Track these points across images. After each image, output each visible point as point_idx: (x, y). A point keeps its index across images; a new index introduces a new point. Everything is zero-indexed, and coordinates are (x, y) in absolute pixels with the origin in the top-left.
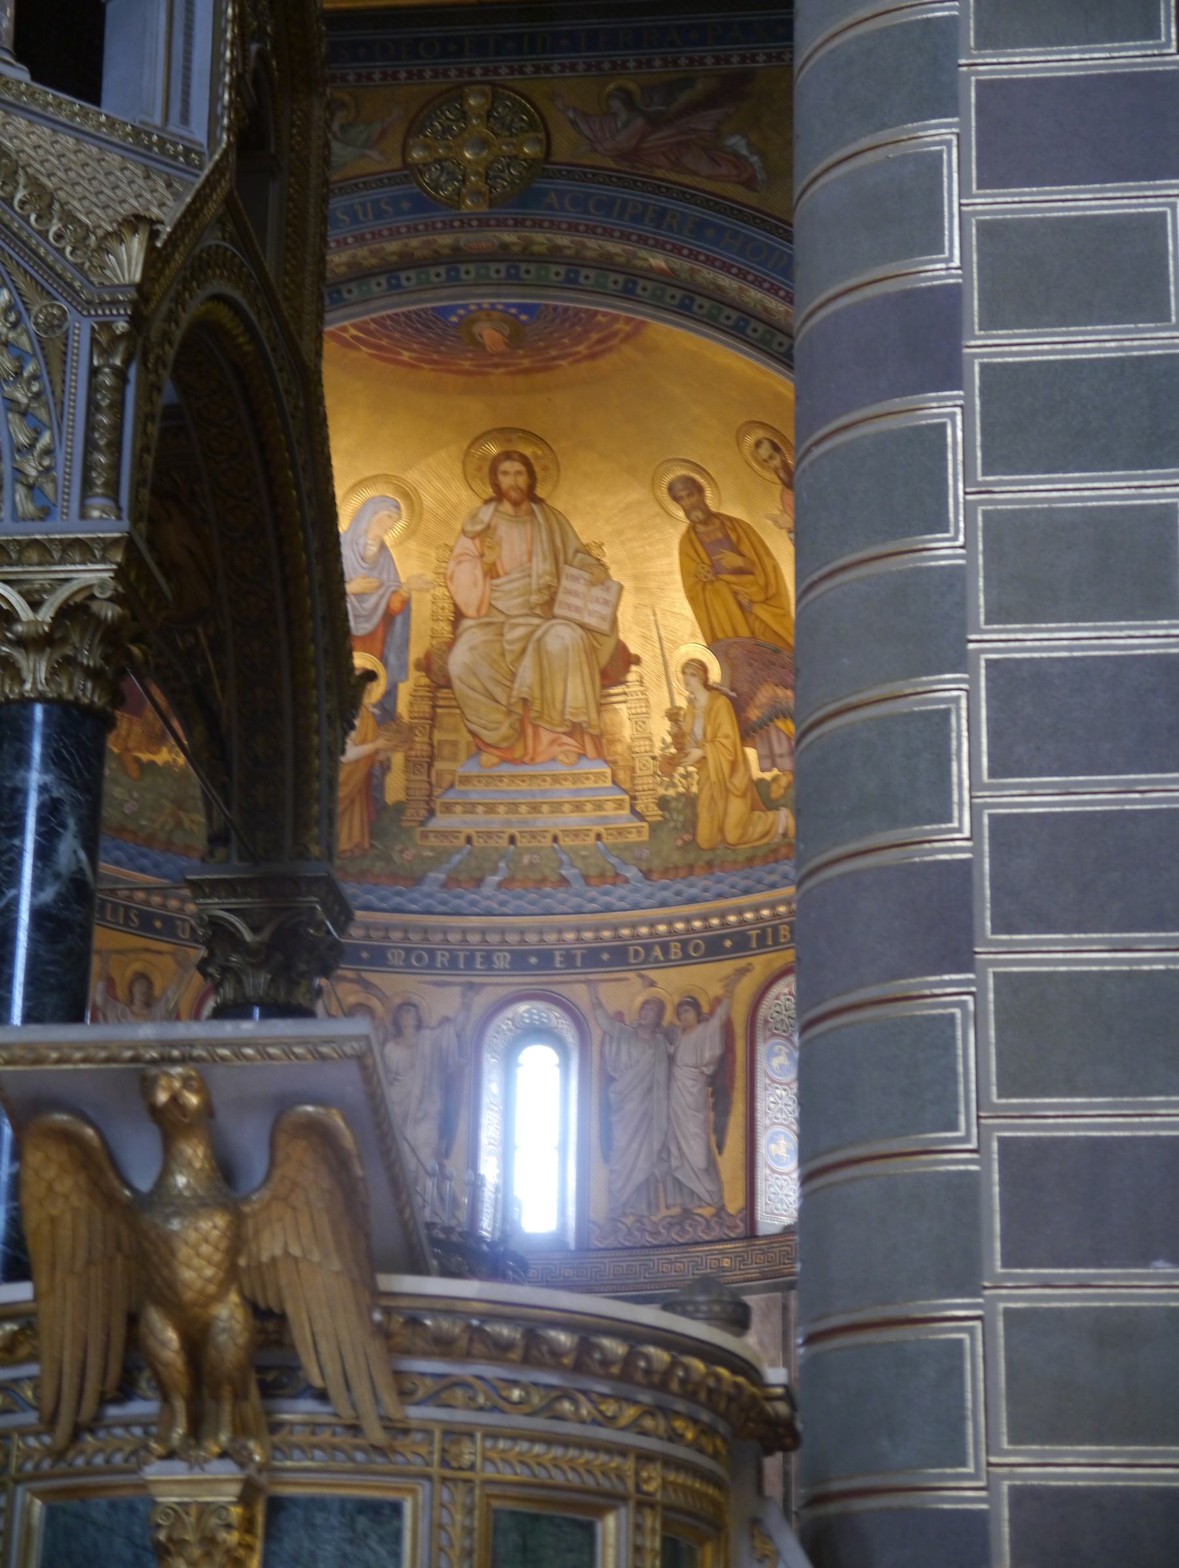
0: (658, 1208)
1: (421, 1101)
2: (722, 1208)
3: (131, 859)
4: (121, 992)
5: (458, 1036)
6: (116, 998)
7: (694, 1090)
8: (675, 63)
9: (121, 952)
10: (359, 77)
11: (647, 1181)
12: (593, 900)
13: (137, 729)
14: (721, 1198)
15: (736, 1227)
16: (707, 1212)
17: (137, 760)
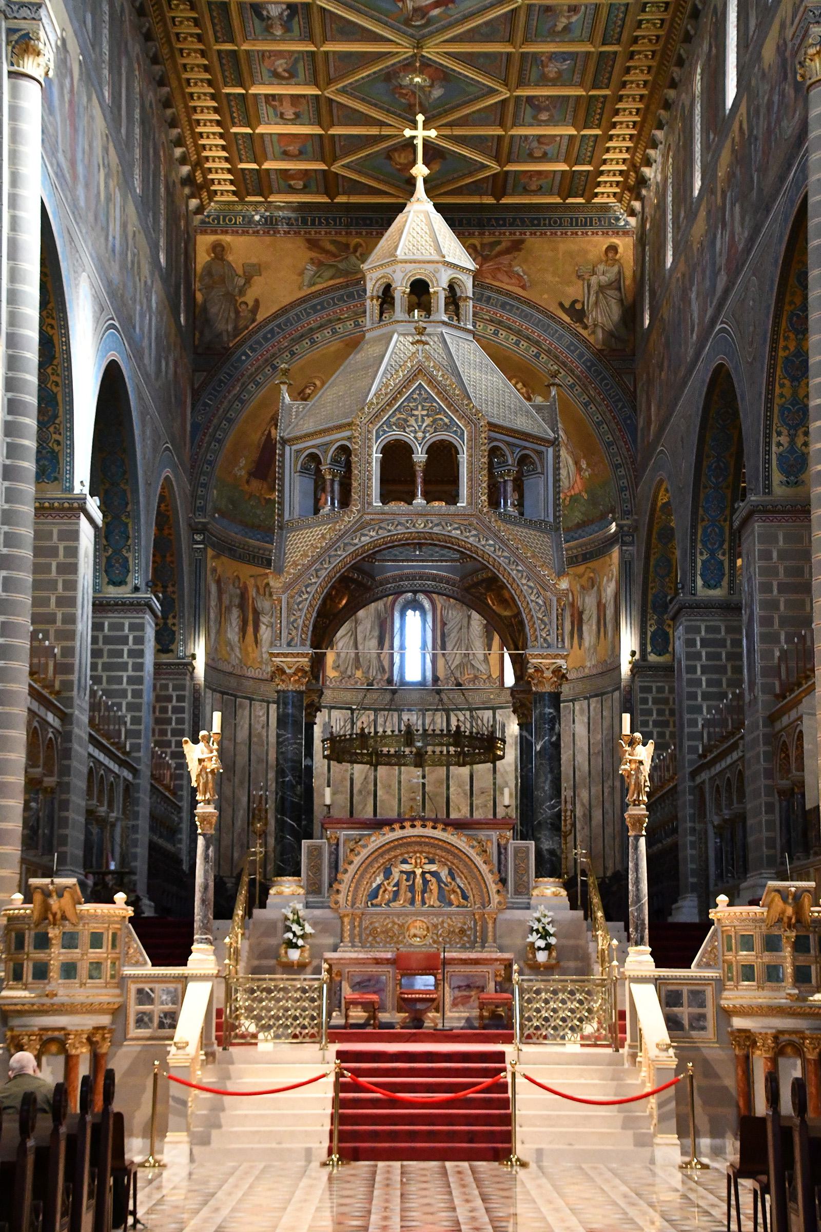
4: (261, 591)
16: (485, 677)
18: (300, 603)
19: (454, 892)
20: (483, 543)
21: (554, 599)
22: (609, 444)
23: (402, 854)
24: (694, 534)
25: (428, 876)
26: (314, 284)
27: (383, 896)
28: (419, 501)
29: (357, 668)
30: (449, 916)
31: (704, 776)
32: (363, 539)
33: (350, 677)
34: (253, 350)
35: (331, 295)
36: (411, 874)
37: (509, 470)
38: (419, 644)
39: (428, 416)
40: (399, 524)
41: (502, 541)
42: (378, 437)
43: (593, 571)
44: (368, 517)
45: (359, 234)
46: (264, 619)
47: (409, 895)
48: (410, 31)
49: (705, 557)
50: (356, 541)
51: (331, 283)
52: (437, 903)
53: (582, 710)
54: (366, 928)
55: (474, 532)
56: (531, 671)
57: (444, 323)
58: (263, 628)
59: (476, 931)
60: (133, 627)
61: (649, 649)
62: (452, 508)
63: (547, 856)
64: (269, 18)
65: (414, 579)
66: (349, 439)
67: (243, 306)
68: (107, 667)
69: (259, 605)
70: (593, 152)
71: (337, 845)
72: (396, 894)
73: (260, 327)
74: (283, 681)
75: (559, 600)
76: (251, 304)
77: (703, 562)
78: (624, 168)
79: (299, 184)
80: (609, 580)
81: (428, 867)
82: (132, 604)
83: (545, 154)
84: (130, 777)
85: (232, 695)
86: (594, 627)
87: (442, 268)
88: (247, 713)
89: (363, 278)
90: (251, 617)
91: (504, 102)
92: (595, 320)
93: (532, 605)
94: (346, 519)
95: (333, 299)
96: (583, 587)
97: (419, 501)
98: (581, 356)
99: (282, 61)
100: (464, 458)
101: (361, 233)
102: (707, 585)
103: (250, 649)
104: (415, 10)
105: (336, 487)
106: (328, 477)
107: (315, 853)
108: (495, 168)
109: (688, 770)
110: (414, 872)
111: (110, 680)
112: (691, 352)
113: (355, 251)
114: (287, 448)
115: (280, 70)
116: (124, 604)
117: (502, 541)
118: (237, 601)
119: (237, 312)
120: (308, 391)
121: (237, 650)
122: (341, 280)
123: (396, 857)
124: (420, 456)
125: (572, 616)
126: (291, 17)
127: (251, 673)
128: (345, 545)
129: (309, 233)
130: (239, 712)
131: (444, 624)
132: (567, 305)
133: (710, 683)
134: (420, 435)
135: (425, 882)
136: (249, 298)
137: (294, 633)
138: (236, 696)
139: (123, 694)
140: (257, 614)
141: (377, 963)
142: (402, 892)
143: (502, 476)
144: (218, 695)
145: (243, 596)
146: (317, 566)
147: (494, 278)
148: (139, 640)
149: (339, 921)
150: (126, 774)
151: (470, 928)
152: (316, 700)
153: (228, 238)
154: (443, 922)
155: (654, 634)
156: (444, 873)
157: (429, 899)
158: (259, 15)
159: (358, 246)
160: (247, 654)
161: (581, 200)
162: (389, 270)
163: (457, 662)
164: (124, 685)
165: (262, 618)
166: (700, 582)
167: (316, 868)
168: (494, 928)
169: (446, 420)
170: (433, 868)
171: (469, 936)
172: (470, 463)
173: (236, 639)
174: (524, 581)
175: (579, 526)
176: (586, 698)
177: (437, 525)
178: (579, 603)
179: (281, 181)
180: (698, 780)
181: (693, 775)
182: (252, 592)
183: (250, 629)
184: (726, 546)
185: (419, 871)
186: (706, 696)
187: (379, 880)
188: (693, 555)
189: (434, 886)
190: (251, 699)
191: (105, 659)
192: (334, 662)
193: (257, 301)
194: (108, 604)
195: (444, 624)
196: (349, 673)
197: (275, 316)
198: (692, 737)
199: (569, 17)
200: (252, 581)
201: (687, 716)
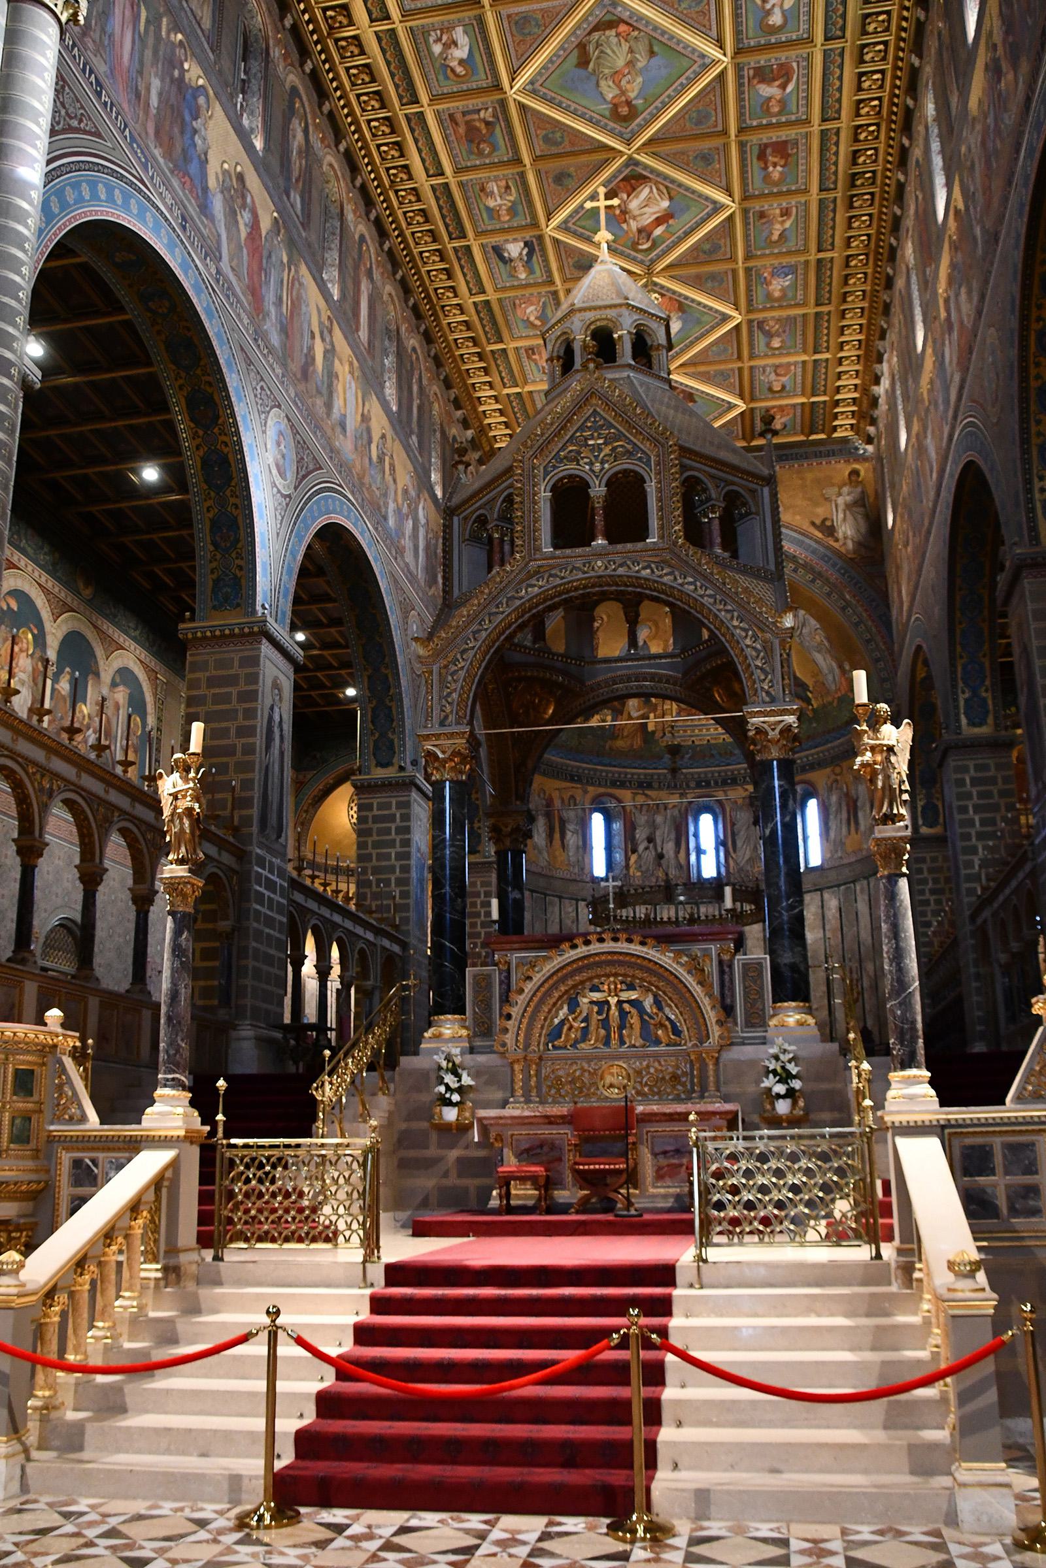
18: (456, 672)
19: (662, 1025)
21: (776, 642)
22: (868, 641)
23: (590, 979)
24: (954, 672)
25: (626, 1006)
27: (567, 1035)
30: (656, 1056)
31: (987, 913)
36: (603, 1005)
37: (713, 506)
39: (605, 444)
40: (574, 568)
41: (705, 577)
42: (546, 473)
46: (571, 827)
47: (602, 1032)
48: (640, 256)
49: (967, 695)
52: (639, 1042)
53: (862, 890)
54: (547, 1077)
56: (751, 734)
57: (630, 366)
58: (569, 835)
59: (693, 1076)
60: (400, 805)
61: (920, 822)
62: (640, 545)
63: (787, 973)
64: (511, 260)
65: (629, 680)
68: (377, 845)
69: (565, 814)
71: (509, 971)
72: (585, 1032)
74: (437, 769)
75: (783, 643)
77: (966, 701)
78: (856, 395)
81: (625, 996)
82: (397, 783)
83: (784, 387)
84: (396, 949)
88: (557, 909)
93: (749, 651)
99: (532, 308)
100: (651, 487)
102: (972, 724)
104: (640, 231)
107: (483, 984)
109: (967, 913)
110: (607, 1002)
111: (380, 857)
112: (932, 494)
114: (455, 519)
115: (532, 319)
116: (390, 784)
117: (705, 577)
121: (545, 855)
123: (582, 982)
124: (598, 490)
126: (530, 254)
127: (559, 874)
128: (509, 599)
130: (550, 909)
131: (733, 824)
132: (818, 522)
133: (983, 822)
135: (623, 1014)
137: (448, 709)
139: (392, 869)
140: (563, 823)
141: (551, 1123)
142: (592, 1028)
146: (475, 627)
148: (406, 817)
149: (508, 1070)
150: (386, 943)
151: (685, 1074)
154: (648, 1067)
155: (923, 808)
156: (648, 1002)
157: (630, 1036)
158: (501, 258)
160: (555, 857)
161: (823, 436)
162: (568, 324)
163: (747, 857)
164: (393, 861)
166: (964, 721)
167: (485, 1004)
168: (717, 1071)
169: (629, 447)
170: (633, 995)
171: (684, 1085)
172: (659, 490)
174: (735, 623)
177: (621, 565)
178: (853, 792)
180: (979, 921)
181: (973, 918)
182: (557, 803)
183: (557, 836)
184: (988, 682)
185: (613, 1001)
186: (981, 836)
187: (562, 1014)
188: (956, 693)
189: (635, 1020)
190: (560, 898)
191: (375, 838)
194: (376, 785)
195: (733, 824)
198: (970, 878)
199: (783, 222)
201: (962, 858)
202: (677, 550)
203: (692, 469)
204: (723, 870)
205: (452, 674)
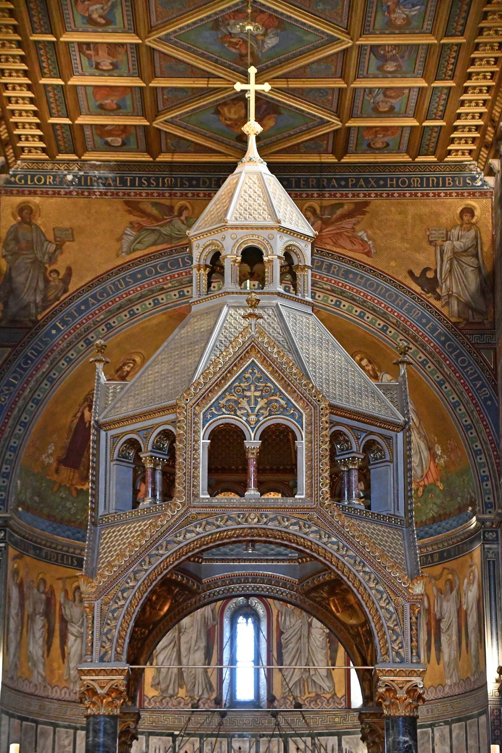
0: (305, 694)
1: (197, 641)
2: (335, 694)
3: (73, 534)
4: (71, 596)
5: (212, 611)
6: (68, 599)
7: (321, 639)
8: (335, 196)
9: (70, 578)
10: (193, 195)
11: (299, 680)
12: (273, 550)
13: (77, 475)
14: (334, 690)
15: (342, 703)
16: (328, 696)
17: (76, 489)
20: (325, 540)
21: (407, 606)
22: (468, 428)
26: (134, 250)
28: (252, 492)
29: (181, 686)
32: (188, 535)
33: (171, 697)
34: (64, 323)
35: (153, 263)
37: (354, 458)
38: (251, 656)
39: (262, 397)
40: (229, 518)
42: (205, 421)
43: (452, 572)
44: (193, 511)
45: (184, 196)
46: (73, 629)
50: (181, 538)
51: (154, 249)
53: (442, 736)
55: (314, 528)
56: (382, 690)
57: (279, 294)
58: (71, 639)
62: (290, 500)
65: (246, 581)
66: (173, 423)
67: (54, 275)
69: (67, 612)
70: (445, 106)
73: (72, 299)
74: (94, 703)
75: (412, 607)
76: (62, 272)
78: (481, 123)
79: (118, 141)
80: (470, 583)
83: (392, 108)
85: (33, 721)
86: (454, 638)
87: (278, 236)
89: (189, 245)
90: (57, 626)
91: (345, 52)
92: (449, 290)
93: (382, 612)
94: (169, 513)
95: (155, 267)
96: (440, 591)
97: (252, 492)
98: (434, 330)
100: (302, 445)
101: (186, 195)
103: (55, 665)
105: (158, 477)
106: (149, 466)
108: (337, 124)
113: (180, 215)
114: (103, 433)
117: (347, 540)
118: (41, 608)
119: (47, 281)
120: (126, 368)
121: (41, 668)
122: (164, 246)
125: (429, 624)
127: (56, 693)
129: (129, 194)
130: (41, 742)
131: (281, 633)
132: (417, 273)
134: (253, 418)
136: (61, 265)
137: (108, 645)
138: (37, 722)
140: (64, 622)
143: (345, 465)
144: (17, 721)
145: (49, 602)
146: (135, 567)
147: (335, 244)
152: (132, 725)
153: (37, 200)
159: (182, 209)
160: (52, 671)
161: (432, 159)
162: (218, 237)
163: (295, 678)
165: (69, 627)
169: (283, 402)
172: (310, 450)
173: (40, 653)
174: (372, 585)
175: (434, 520)
176: (446, 723)
177: (272, 520)
179: (97, 139)
182: (60, 597)
183: (56, 641)
190: (55, 726)
192: (154, 679)
193: (69, 271)
195: (280, 633)
196: (170, 691)
197: (90, 286)
200: (60, 583)
202: (323, 510)
203: (338, 424)
204: (263, 692)
205: (113, 611)
